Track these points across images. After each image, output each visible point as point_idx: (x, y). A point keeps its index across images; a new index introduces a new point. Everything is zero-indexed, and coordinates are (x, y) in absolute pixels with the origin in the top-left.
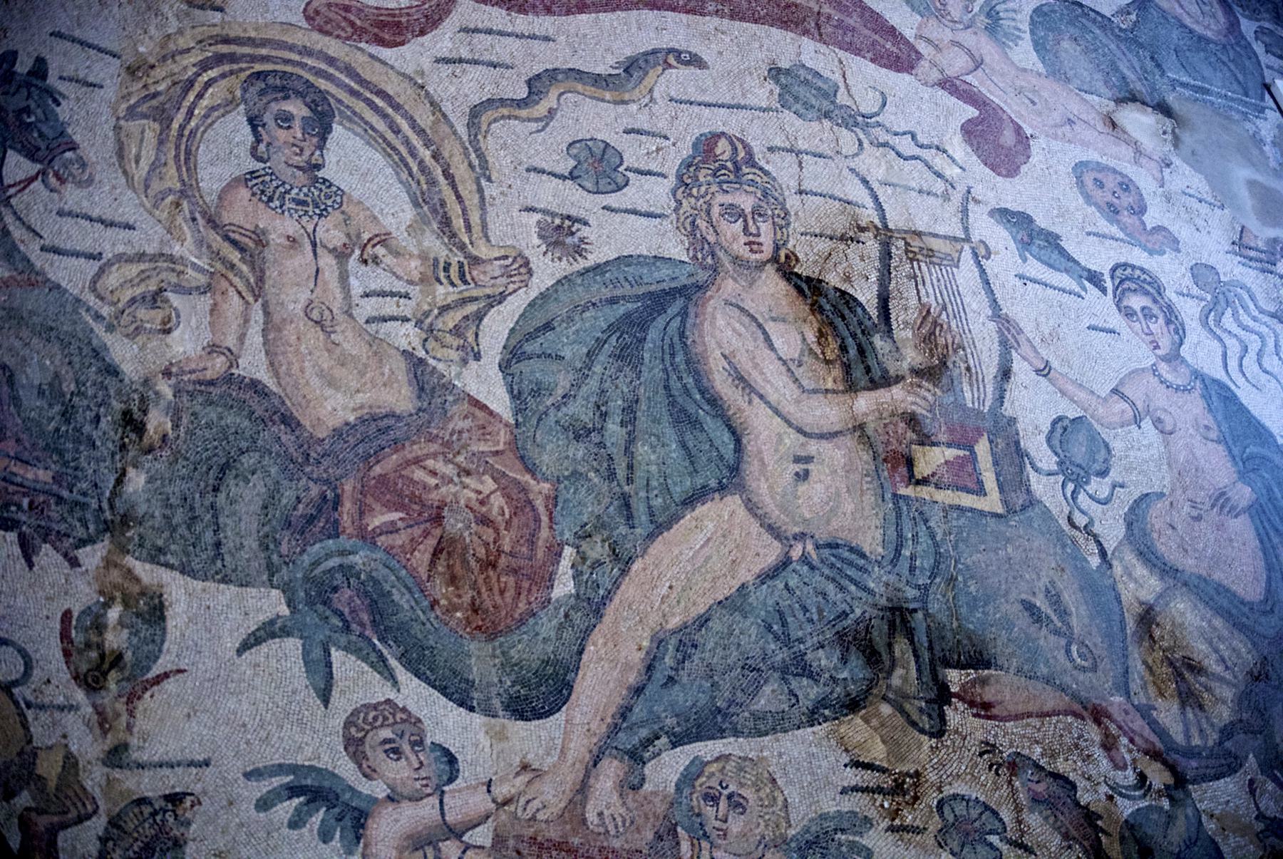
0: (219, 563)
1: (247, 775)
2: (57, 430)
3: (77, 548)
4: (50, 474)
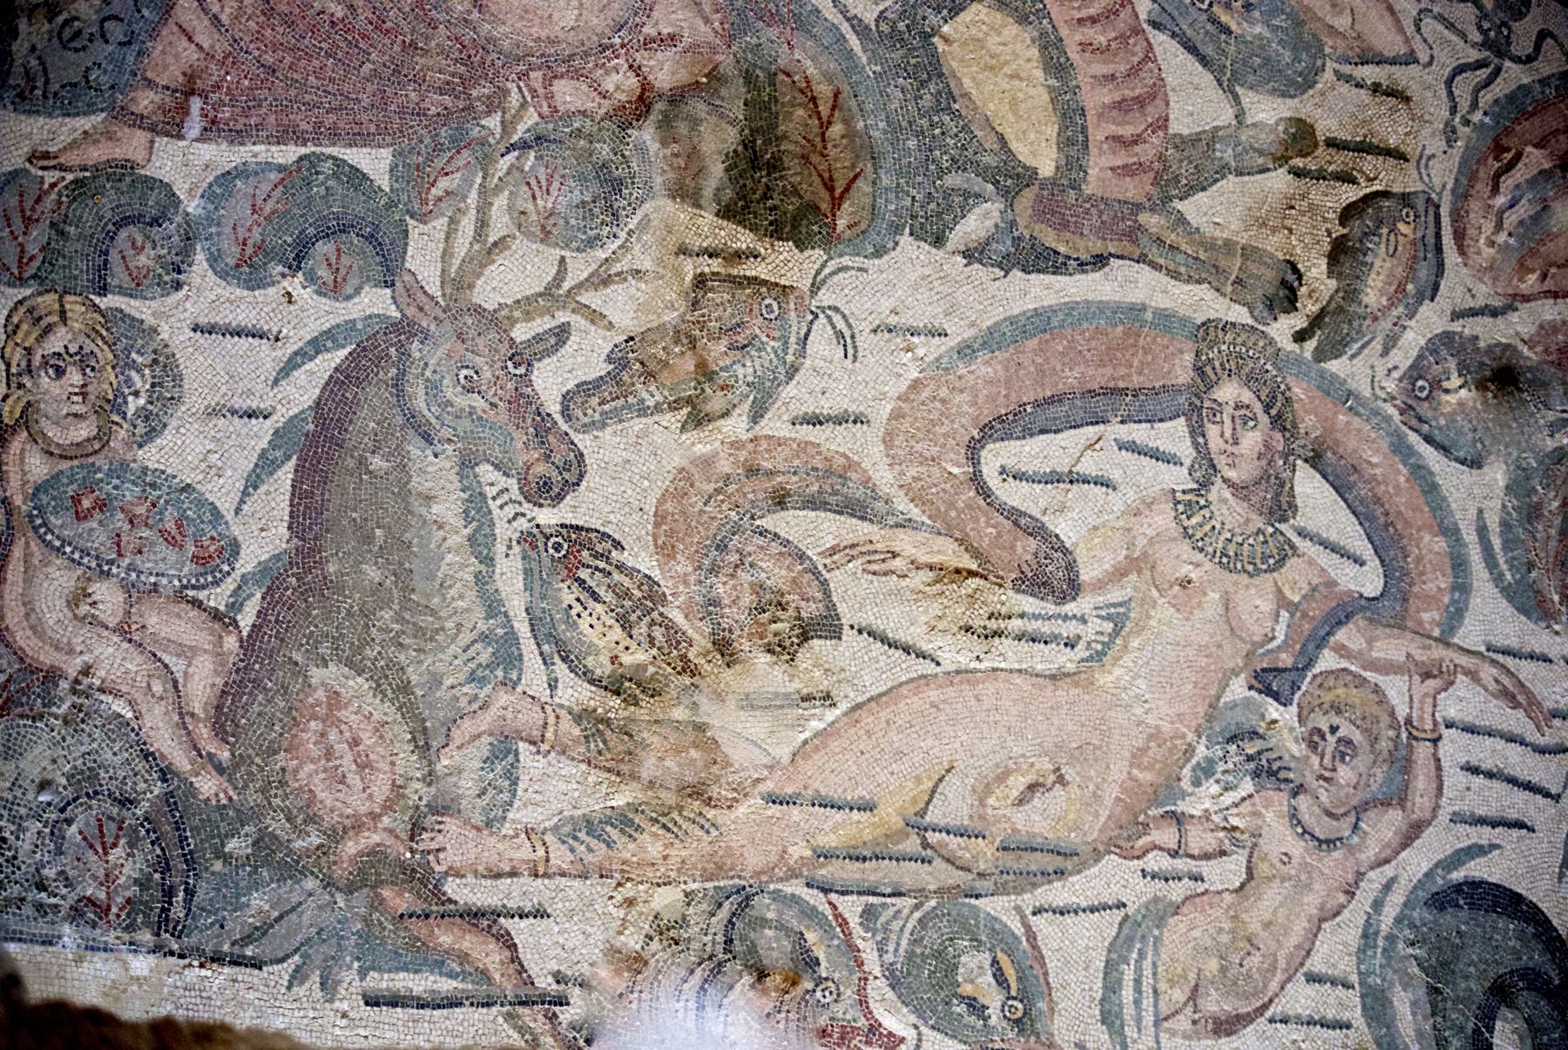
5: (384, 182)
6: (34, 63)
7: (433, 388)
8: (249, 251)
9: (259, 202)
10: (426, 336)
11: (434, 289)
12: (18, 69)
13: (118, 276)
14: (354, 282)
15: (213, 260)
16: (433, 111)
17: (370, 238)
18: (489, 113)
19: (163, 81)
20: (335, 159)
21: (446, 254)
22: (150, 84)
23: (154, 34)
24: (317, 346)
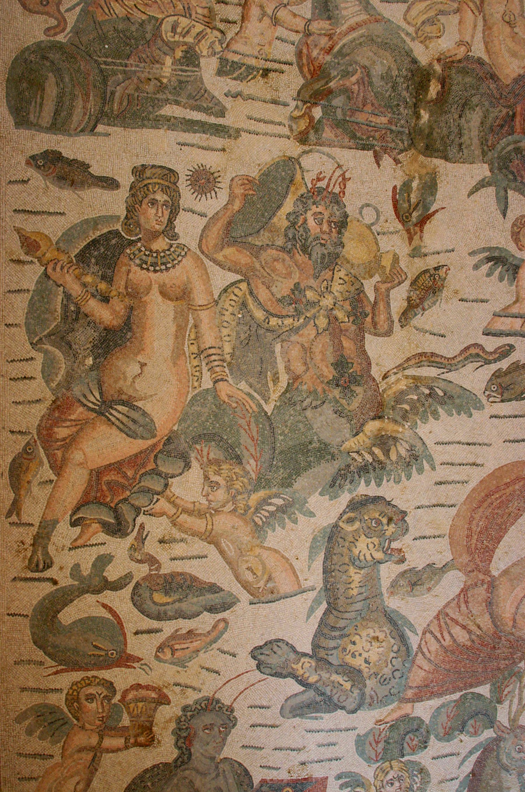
0: (461, 153)
1: (470, 254)
2: (390, 96)
3: (399, 154)
4: (387, 118)
5: (488, 695)
6: (373, 693)
7: (508, 755)
8: (447, 730)
9: (449, 714)
10: (505, 739)
11: (507, 724)
12: (368, 697)
13: (407, 749)
14: (480, 730)
15: (436, 736)
16: (502, 667)
17: (485, 715)
18: (520, 662)
19: (414, 685)
20: (472, 693)
21: (509, 713)
22: (411, 687)
23: (410, 671)
24: (471, 753)
